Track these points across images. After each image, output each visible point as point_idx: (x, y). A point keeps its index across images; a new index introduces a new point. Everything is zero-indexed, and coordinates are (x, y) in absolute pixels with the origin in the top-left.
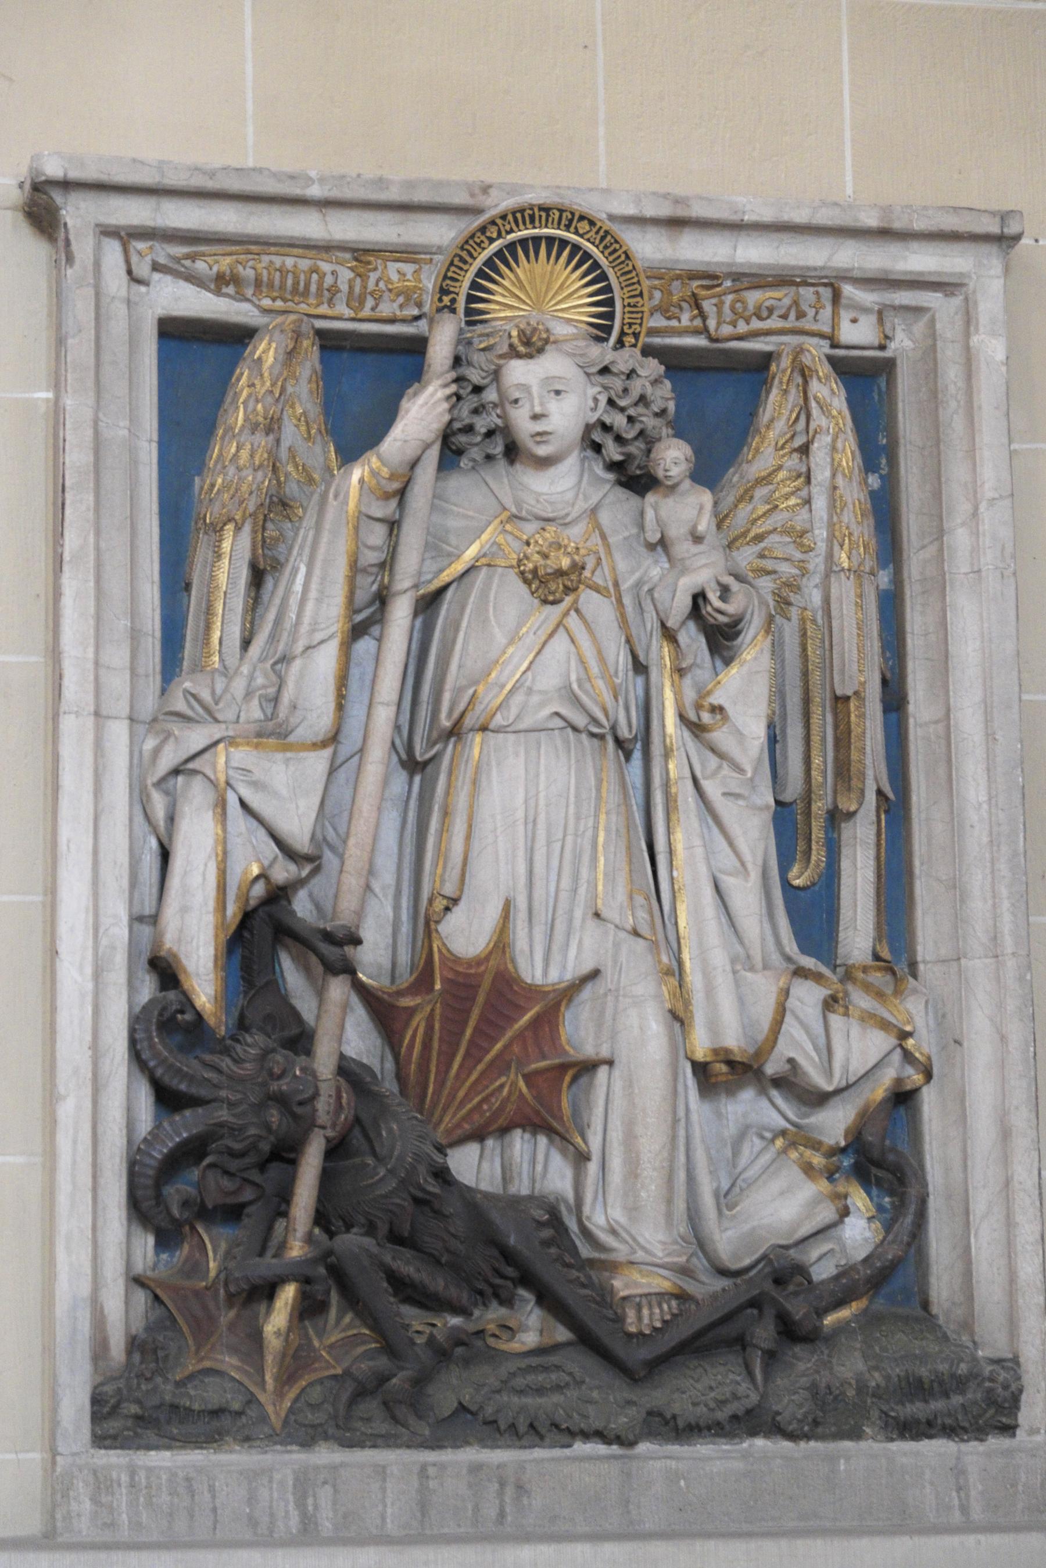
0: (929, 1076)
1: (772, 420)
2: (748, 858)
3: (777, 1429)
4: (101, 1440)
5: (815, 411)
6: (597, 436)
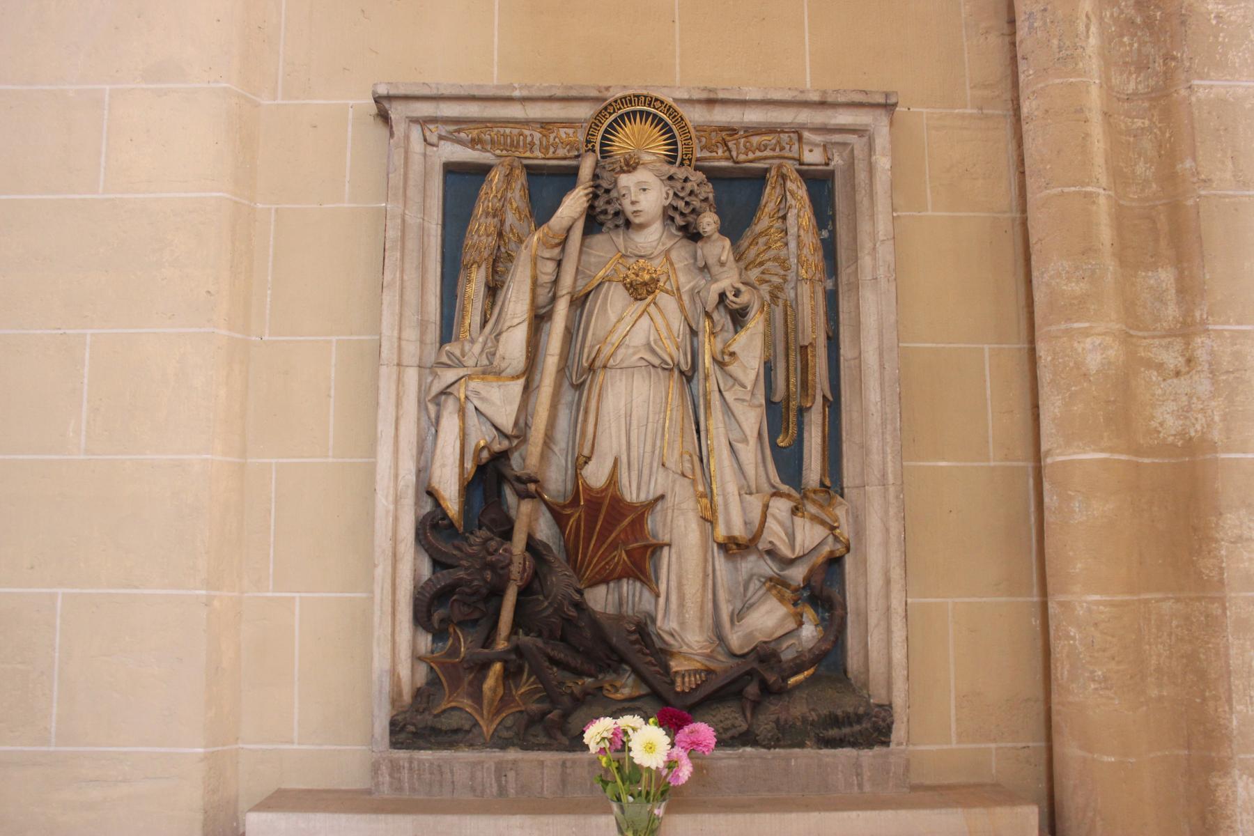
0: (848, 550)
1: (766, 203)
2: (748, 432)
3: (755, 743)
4: (395, 744)
5: (789, 197)
6: (671, 213)
